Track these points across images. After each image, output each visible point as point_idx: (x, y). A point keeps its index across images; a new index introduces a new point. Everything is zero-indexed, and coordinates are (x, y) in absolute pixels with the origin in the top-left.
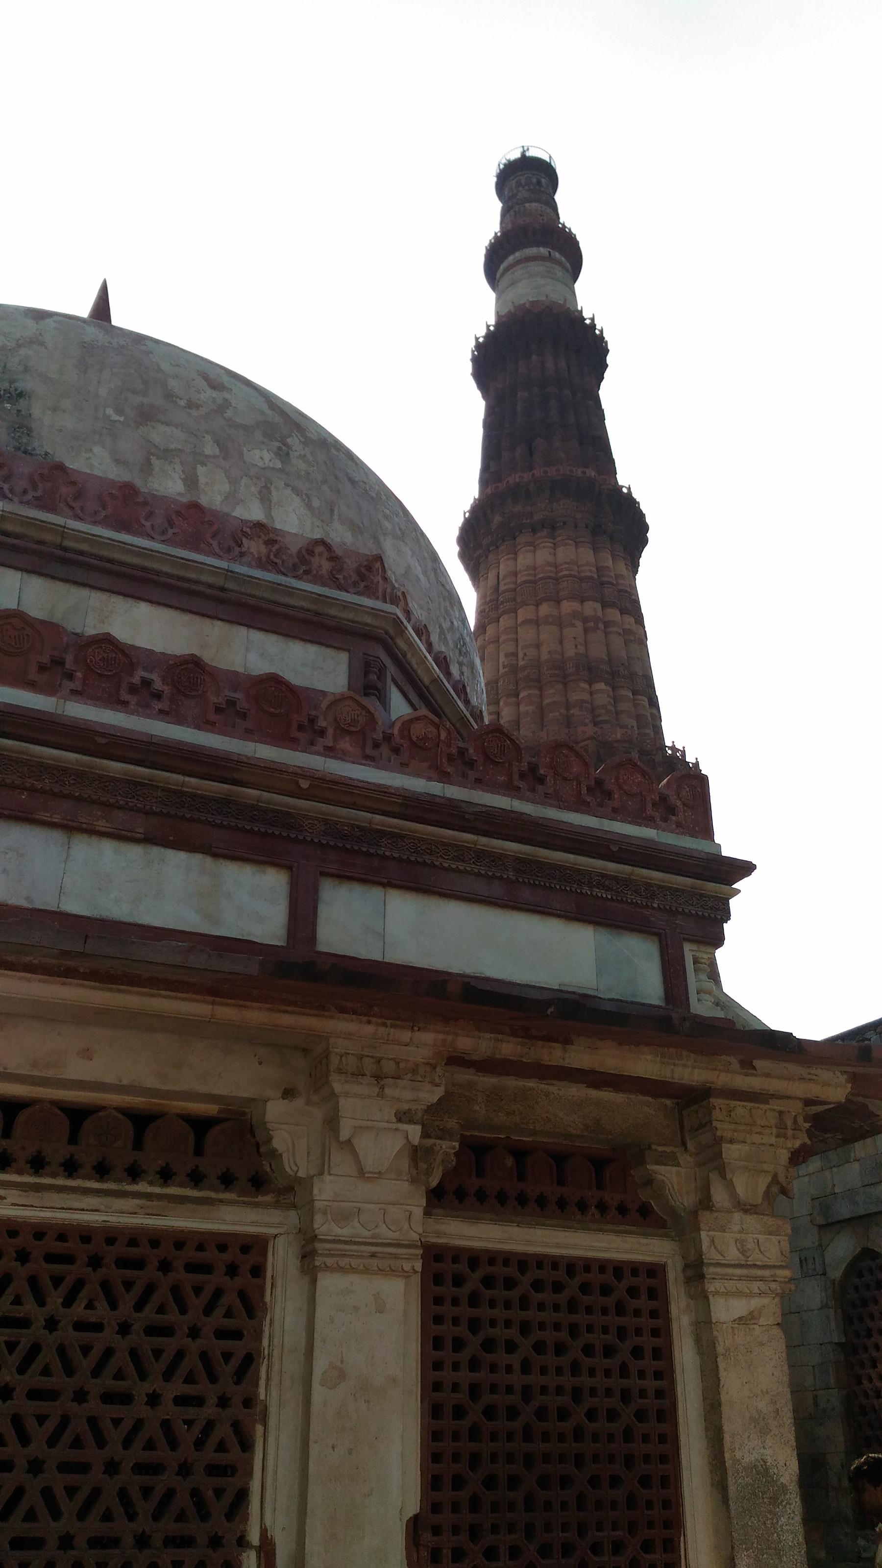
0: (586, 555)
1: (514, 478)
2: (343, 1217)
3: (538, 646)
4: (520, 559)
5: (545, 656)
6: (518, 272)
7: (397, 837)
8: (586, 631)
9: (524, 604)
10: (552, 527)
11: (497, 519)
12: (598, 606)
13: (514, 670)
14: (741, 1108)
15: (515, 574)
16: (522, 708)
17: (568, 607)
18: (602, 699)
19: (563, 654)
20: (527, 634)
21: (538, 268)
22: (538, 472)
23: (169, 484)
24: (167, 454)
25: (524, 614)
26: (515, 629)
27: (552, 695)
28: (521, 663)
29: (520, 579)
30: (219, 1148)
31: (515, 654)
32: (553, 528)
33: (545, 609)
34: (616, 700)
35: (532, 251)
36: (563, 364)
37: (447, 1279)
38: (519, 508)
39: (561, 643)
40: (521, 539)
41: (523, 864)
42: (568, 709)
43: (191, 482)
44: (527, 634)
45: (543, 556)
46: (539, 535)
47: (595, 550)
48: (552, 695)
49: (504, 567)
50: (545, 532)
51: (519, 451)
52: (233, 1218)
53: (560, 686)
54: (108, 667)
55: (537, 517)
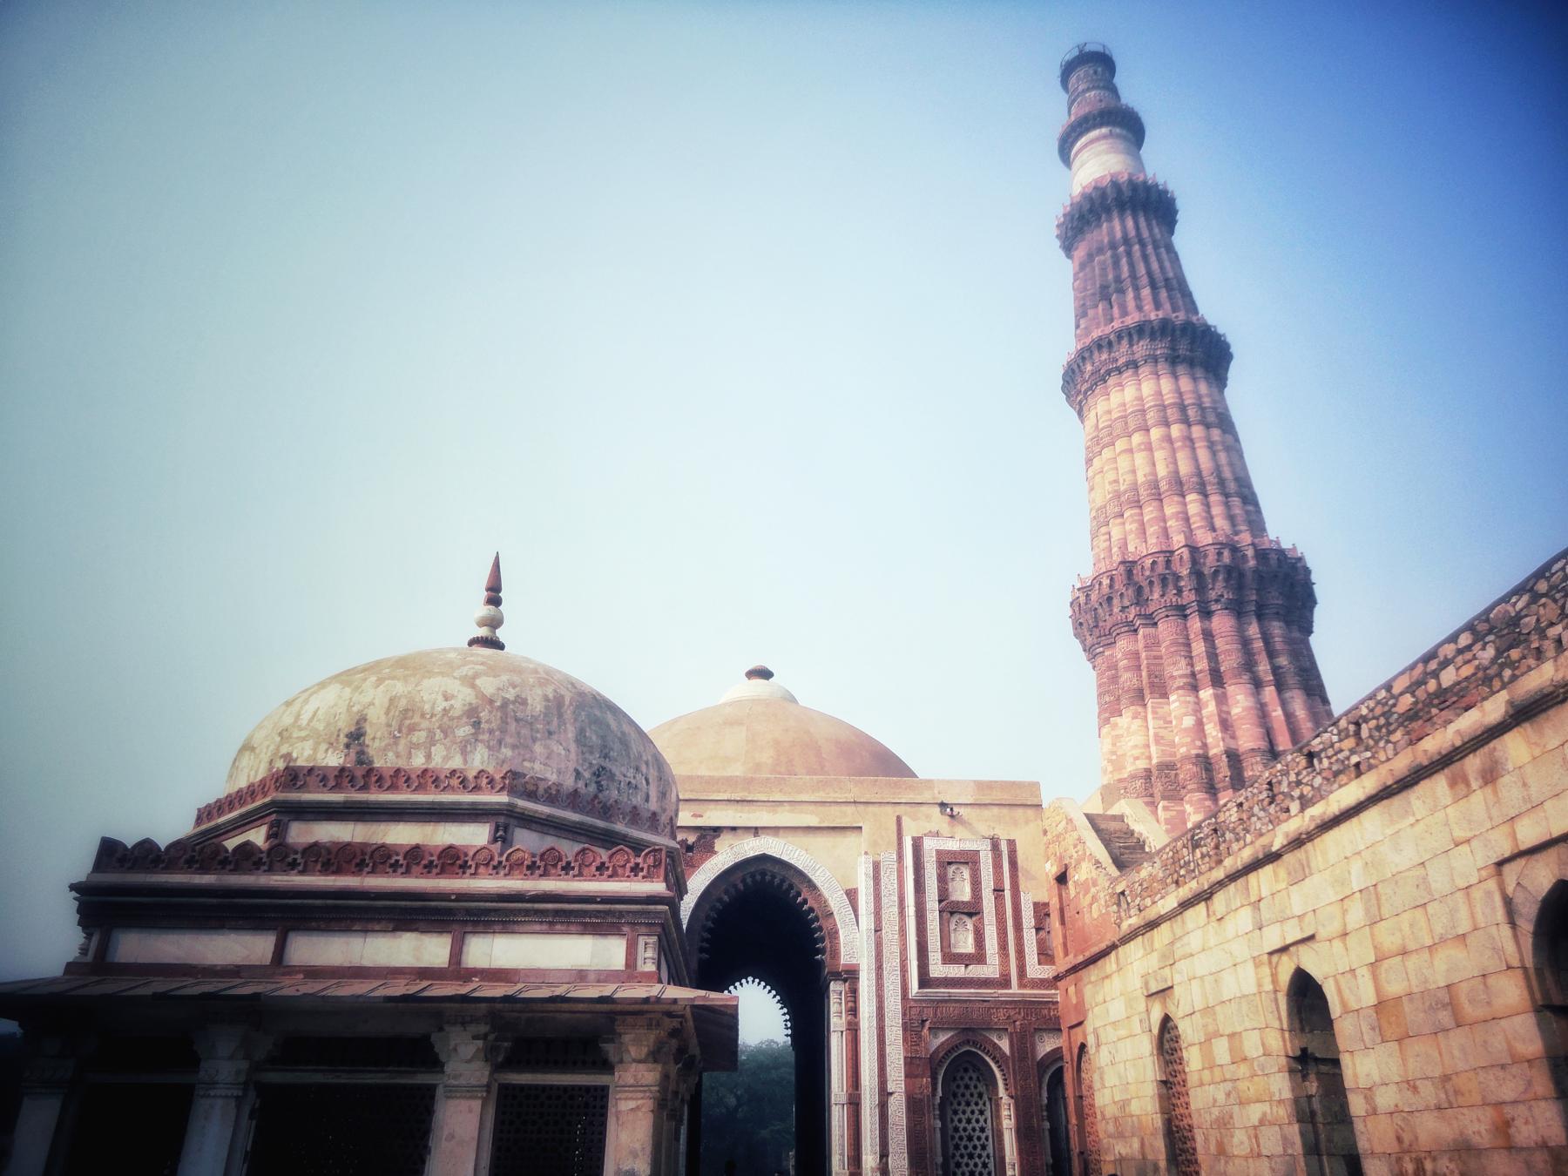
0: (1166, 384)
1: (1096, 334)
2: (455, 1077)
3: (1134, 472)
6: (1085, 155)
7: (496, 910)
8: (1174, 451)
9: (1119, 437)
10: (1133, 365)
11: (1089, 368)
12: (1182, 426)
13: (1117, 495)
14: (630, 1019)
15: (1109, 412)
16: (1128, 527)
17: (1156, 433)
19: (1155, 475)
20: (1124, 463)
22: (1116, 324)
23: (418, 761)
24: (417, 746)
25: (1121, 445)
26: (1114, 460)
27: (1149, 512)
28: (1122, 488)
29: (1115, 415)
31: (1116, 481)
32: (1137, 367)
33: (1137, 438)
36: (1130, 223)
38: (1104, 356)
39: (1154, 465)
40: (1111, 381)
41: (557, 913)
42: (1165, 521)
43: (428, 757)
44: (1124, 463)
45: (1129, 393)
46: (1125, 375)
48: (1149, 512)
50: (1130, 372)
52: (422, 1079)
53: (1155, 504)
54: (380, 858)
55: (1121, 361)
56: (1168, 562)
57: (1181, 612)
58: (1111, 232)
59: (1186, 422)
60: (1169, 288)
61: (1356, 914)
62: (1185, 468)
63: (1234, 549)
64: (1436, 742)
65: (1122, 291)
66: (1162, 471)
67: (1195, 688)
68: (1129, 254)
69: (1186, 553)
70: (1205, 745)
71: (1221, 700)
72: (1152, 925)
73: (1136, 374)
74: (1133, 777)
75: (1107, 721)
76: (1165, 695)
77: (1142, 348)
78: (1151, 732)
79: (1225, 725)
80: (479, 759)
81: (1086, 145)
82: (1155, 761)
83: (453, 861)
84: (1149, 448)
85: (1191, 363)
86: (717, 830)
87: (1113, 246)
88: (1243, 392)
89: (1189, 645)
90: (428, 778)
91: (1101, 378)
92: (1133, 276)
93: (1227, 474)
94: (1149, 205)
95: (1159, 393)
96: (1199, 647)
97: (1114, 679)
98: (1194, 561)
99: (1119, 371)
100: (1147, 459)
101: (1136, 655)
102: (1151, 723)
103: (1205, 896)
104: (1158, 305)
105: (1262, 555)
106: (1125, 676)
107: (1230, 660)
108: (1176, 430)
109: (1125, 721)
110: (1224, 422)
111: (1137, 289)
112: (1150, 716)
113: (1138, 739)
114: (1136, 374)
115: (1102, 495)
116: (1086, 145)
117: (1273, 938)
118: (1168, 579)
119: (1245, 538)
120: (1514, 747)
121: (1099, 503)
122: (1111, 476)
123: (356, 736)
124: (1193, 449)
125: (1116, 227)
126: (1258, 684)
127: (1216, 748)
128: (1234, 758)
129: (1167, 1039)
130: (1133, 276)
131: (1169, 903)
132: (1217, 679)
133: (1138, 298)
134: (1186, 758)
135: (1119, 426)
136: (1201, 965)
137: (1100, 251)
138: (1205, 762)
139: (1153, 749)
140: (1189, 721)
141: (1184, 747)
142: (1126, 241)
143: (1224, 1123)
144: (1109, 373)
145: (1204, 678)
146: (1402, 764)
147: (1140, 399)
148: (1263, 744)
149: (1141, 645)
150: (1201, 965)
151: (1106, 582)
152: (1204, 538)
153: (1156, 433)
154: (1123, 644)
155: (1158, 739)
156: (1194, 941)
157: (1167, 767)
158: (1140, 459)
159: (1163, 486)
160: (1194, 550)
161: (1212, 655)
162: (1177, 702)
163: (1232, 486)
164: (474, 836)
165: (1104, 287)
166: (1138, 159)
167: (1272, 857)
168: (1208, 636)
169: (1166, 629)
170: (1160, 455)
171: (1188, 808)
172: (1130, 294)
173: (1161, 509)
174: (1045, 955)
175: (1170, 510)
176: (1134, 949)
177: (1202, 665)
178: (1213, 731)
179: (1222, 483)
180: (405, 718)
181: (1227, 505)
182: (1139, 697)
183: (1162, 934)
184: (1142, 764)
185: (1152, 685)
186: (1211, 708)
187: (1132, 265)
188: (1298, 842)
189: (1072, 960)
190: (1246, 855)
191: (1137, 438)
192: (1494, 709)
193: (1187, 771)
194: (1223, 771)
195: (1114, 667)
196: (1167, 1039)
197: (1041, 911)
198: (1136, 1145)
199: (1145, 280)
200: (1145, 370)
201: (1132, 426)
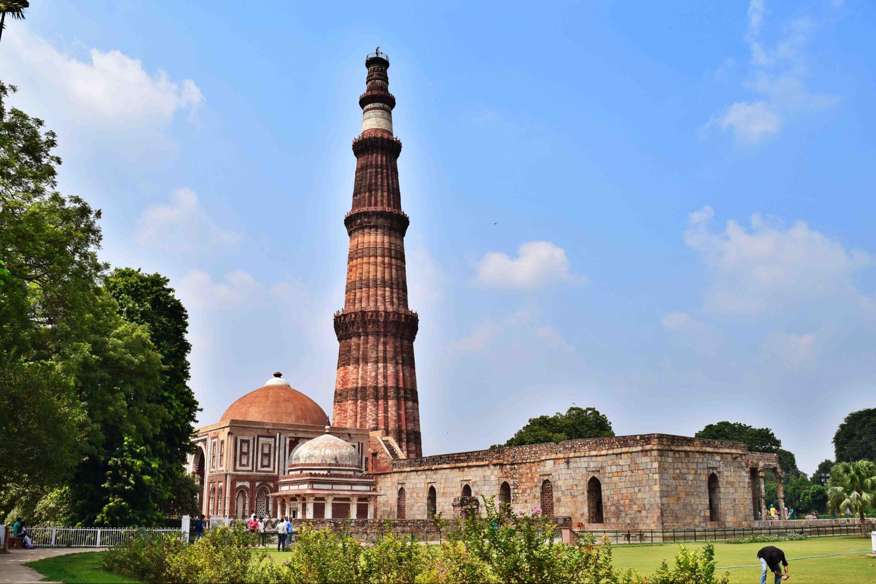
0: (386, 239)
3: (369, 272)
4: (366, 237)
5: (371, 277)
10: (376, 227)
13: (361, 279)
17: (379, 259)
18: (388, 294)
21: (379, 113)
25: (365, 259)
29: (365, 246)
30: (348, 499)
34: (392, 293)
35: (377, 105)
37: (358, 505)
40: (366, 230)
45: (372, 238)
47: (390, 236)
49: (360, 239)
51: (367, 194)
54: (342, 476)
56: (377, 316)
57: (377, 334)
58: (376, 160)
59: (390, 257)
60: (393, 193)
61: (443, 481)
62: (387, 276)
63: (399, 314)
64: (458, 465)
65: (376, 190)
66: (379, 276)
67: (377, 362)
68: (382, 173)
69: (383, 314)
70: (377, 383)
71: (385, 368)
72: (402, 472)
73: (376, 231)
74: (352, 389)
75: (344, 365)
76: (367, 363)
77: (381, 221)
78: (360, 375)
79: (385, 377)
80: (350, 463)
81: (372, 109)
82: (360, 385)
83: (350, 477)
84: (376, 264)
85: (396, 231)
86: (299, 438)
87: (376, 167)
88: (411, 240)
89: (377, 346)
90: (346, 466)
91: (362, 227)
92: (382, 185)
93: (400, 280)
94: (392, 148)
95: (383, 242)
96: (381, 348)
97: (350, 351)
98: (385, 317)
99: (371, 227)
100: (374, 269)
101: (358, 345)
102: (360, 372)
103: (417, 471)
104: (389, 206)
105: (407, 317)
106: (354, 352)
107: (390, 355)
108: (387, 260)
109: (351, 368)
110: (401, 257)
111: (382, 192)
112: (360, 369)
113: (354, 376)
114: (376, 231)
115: (355, 276)
116: (372, 109)
117: (429, 481)
118: (376, 322)
119: (402, 310)
120: (466, 469)
121: (353, 279)
122: (359, 271)
123: (336, 459)
124: (391, 268)
125: (378, 158)
126: (397, 363)
127: (381, 385)
128: (385, 388)
129: (401, 492)
130: (382, 185)
131: (408, 469)
132: (385, 361)
133: (382, 196)
134: (370, 387)
135: (366, 251)
136: (413, 481)
137: (371, 166)
138: (376, 388)
139: (360, 381)
140: (373, 374)
141: (370, 383)
142: (382, 167)
143: (413, 505)
144: (366, 227)
145: (381, 359)
146: (453, 465)
147: (376, 242)
148: (395, 385)
149: (361, 342)
150: (413, 481)
151: (353, 316)
152: (390, 308)
153: (379, 259)
154: (354, 340)
155: (362, 378)
156: (412, 477)
157: (364, 388)
158: (372, 268)
159: (379, 282)
160: (386, 312)
161: (385, 351)
162: (370, 366)
163: (401, 285)
164: (352, 473)
165: (370, 185)
166: (390, 120)
167: (431, 470)
168: (385, 344)
169: (371, 339)
170: (379, 269)
171: (369, 404)
172: (380, 194)
173: (376, 290)
174: (367, 469)
175: (379, 292)
176: (397, 475)
177: (381, 354)
178: (380, 378)
179: (398, 285)
180: (342, 456)
181: (398, 293)
182: (357, 362)
183: (404, 475)
184: (355, 385)
185: (363, 358)
186: (381, 370)
187: (382, 179)
188: (436, 469)
189: (374, 472)
190: (426, 468)
191: (372, 259)
192: (465, 464)
193: (370, 391)
194: (382, 393)
195: (350, 347)
196: (401, 492)
197: (367, 459)
198: (389, 509)
199: (386, 188)
200: (380, 231)
201: (372, 253)
